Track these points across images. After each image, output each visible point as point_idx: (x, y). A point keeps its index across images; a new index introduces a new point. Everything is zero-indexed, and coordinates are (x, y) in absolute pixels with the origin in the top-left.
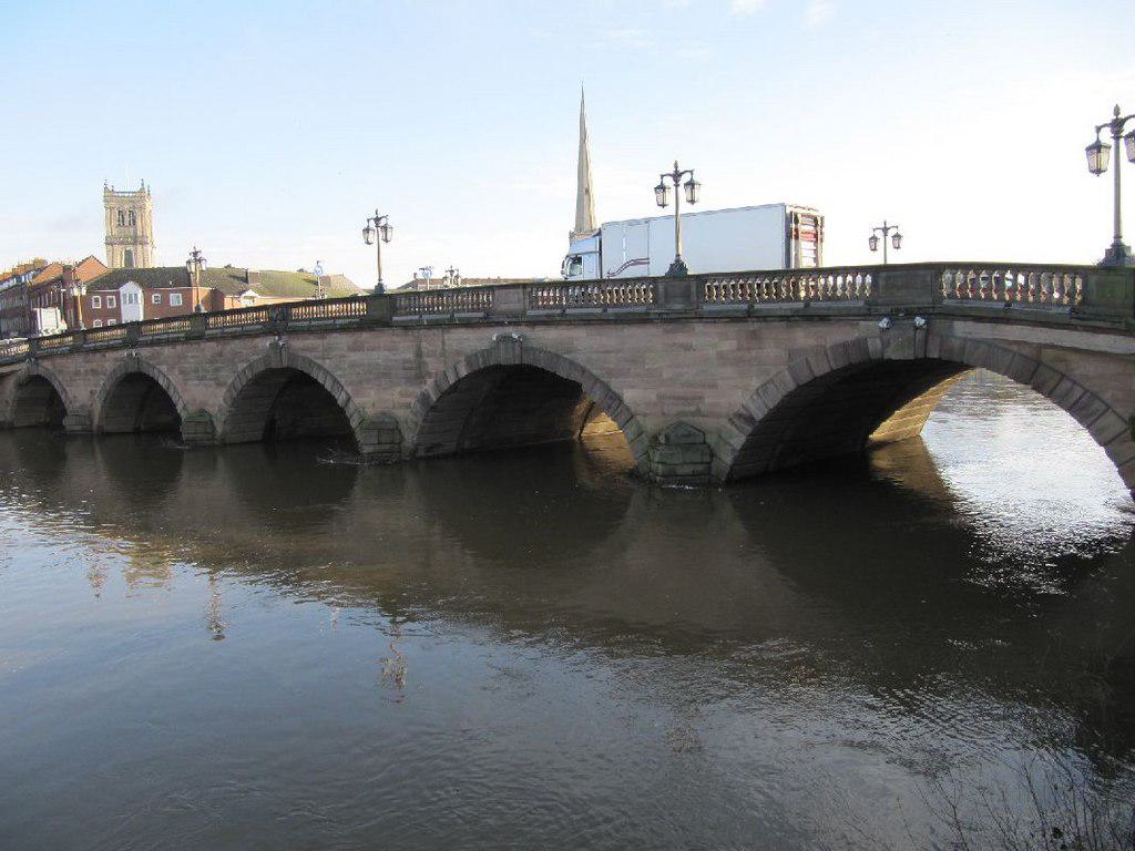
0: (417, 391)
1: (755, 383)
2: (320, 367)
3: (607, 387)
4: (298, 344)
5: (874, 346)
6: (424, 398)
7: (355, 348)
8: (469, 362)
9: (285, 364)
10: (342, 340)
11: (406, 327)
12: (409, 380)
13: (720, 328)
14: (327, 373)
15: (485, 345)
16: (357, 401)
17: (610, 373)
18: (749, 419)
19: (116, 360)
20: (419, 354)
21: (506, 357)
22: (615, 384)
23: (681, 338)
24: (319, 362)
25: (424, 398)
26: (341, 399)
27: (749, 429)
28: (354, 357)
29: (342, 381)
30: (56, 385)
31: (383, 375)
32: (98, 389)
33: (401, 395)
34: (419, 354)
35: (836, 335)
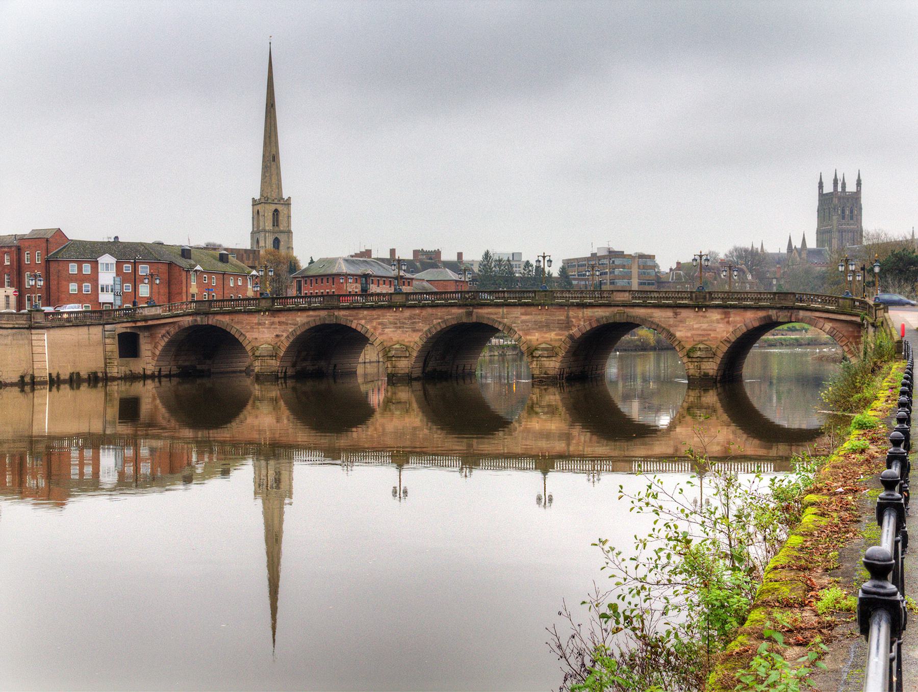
0: (567, 333)
1: (731, 329)
2: (500, 322)
3: (669, 332)
4: (484, 311)
6: (571, 337)
7: (526, 314)
10: (517, 312)
11: (561, 305)
12: (561, 329)
15: (607, 314)
17: (670, 326)
18: (729, 342)
19: (308, 316)
20: (568, 317)
21: (618, 319)
22: (672, 330)
25: (571, 337)
27: (729, 345)
28: (524, 317)
30: (233, 332)
31: (546, 326)
32: (285, 335)
33: (556, 335)
34: (568, 317)
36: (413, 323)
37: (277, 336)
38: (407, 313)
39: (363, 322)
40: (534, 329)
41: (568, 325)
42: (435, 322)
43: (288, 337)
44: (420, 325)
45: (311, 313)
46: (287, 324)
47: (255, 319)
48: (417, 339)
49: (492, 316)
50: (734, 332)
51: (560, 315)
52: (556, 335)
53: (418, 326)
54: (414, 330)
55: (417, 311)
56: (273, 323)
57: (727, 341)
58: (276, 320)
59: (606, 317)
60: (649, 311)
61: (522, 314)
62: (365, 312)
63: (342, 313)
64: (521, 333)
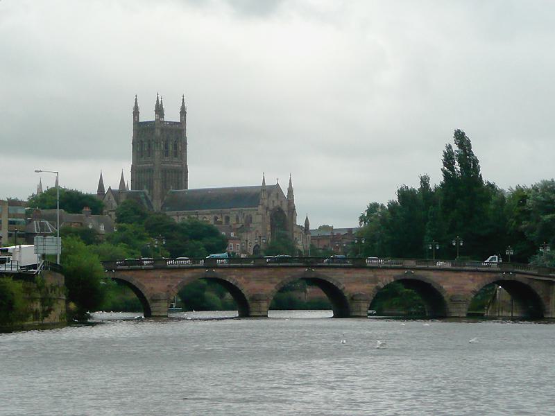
5: (502, 277)
6: (378, 288)
7: (348, 273)
8: (394, 278)
10: (341, 272)
11: (372, 268)
13: (468, 273)
20: (375, 275)
21: (408, 277)
22: (441, 284)
23: (459, 274)
25: (378, 288)
26: (340, 288)
28: (347, 275)
32: (175, 285)
35: (494, 275)
36: (271, 278)
37: (169, 286)
38: (266, 271)
39: (234, 277)
41: (375, 280)
42: (286, 277)
43: (177, 287)
44: (275, 279)
45: (195, 270)
46: (177, 278)
47: (152, 274)
48: (273, 289)
49: (325, 274)
50: (478, 286)
51: (370, 274)
52: (368, 286)
53: (275, 279)
54: (272, 283)
55: (272, 270)
56: (165, 277)
57: (474, 292)
58: (168, 275)
59: (400, 276)
60: (427, 272)
62: (236, 270)
63: (218, 271)
64: (345, 285)
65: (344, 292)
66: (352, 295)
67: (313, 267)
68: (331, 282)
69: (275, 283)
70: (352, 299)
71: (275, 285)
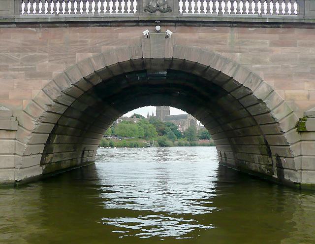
2: (226, 61)
7: (283, 44)
9: (169, 55)
14: (237, 66)
16: (280, 94)
24: (223, 54)
26: (258, 92)
28: (279, 51)
29: (261, 74)
40: (300, 75)
42: (79, 57)
48: (37, 93)
49: (214, 48)
54: (32, 75)
55: (36, 34)
61: (274, 44)
64: (272, 83)
65: (269, 106)
66: (297, 117)
67: (164, 23)
68: (228, 72)
69: (42, 76)
70: (301, 128)
71: (46, 81)
